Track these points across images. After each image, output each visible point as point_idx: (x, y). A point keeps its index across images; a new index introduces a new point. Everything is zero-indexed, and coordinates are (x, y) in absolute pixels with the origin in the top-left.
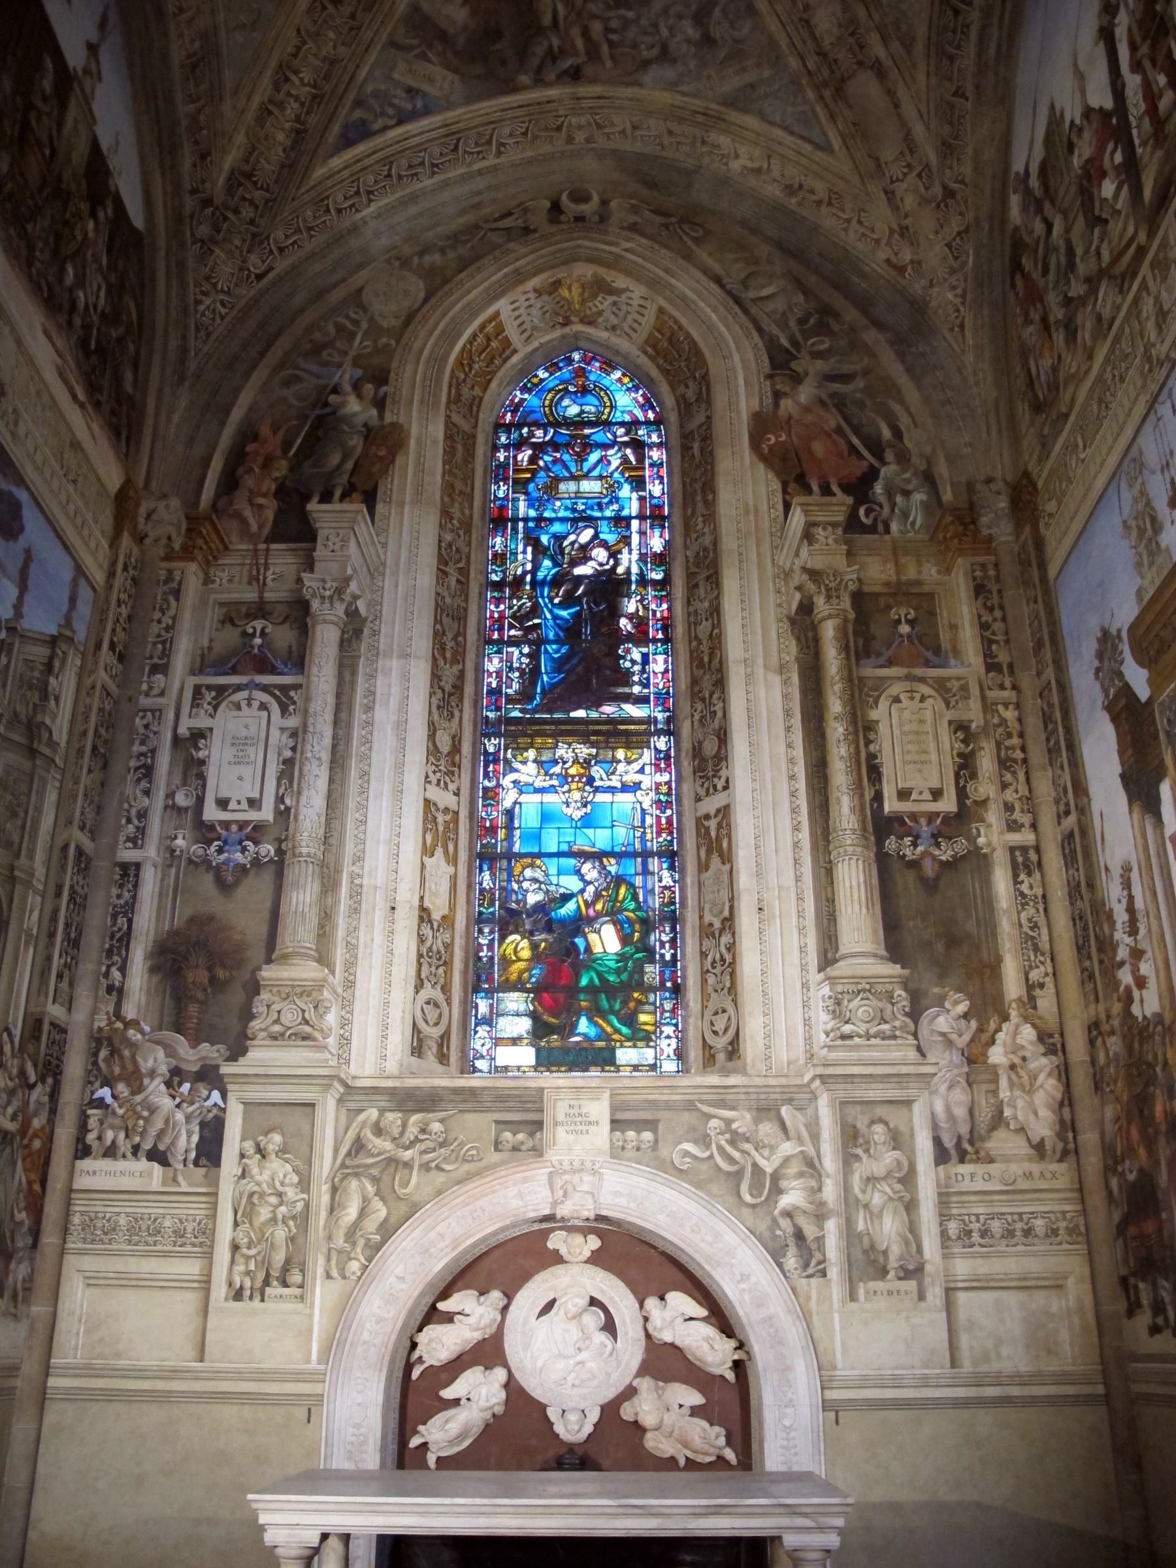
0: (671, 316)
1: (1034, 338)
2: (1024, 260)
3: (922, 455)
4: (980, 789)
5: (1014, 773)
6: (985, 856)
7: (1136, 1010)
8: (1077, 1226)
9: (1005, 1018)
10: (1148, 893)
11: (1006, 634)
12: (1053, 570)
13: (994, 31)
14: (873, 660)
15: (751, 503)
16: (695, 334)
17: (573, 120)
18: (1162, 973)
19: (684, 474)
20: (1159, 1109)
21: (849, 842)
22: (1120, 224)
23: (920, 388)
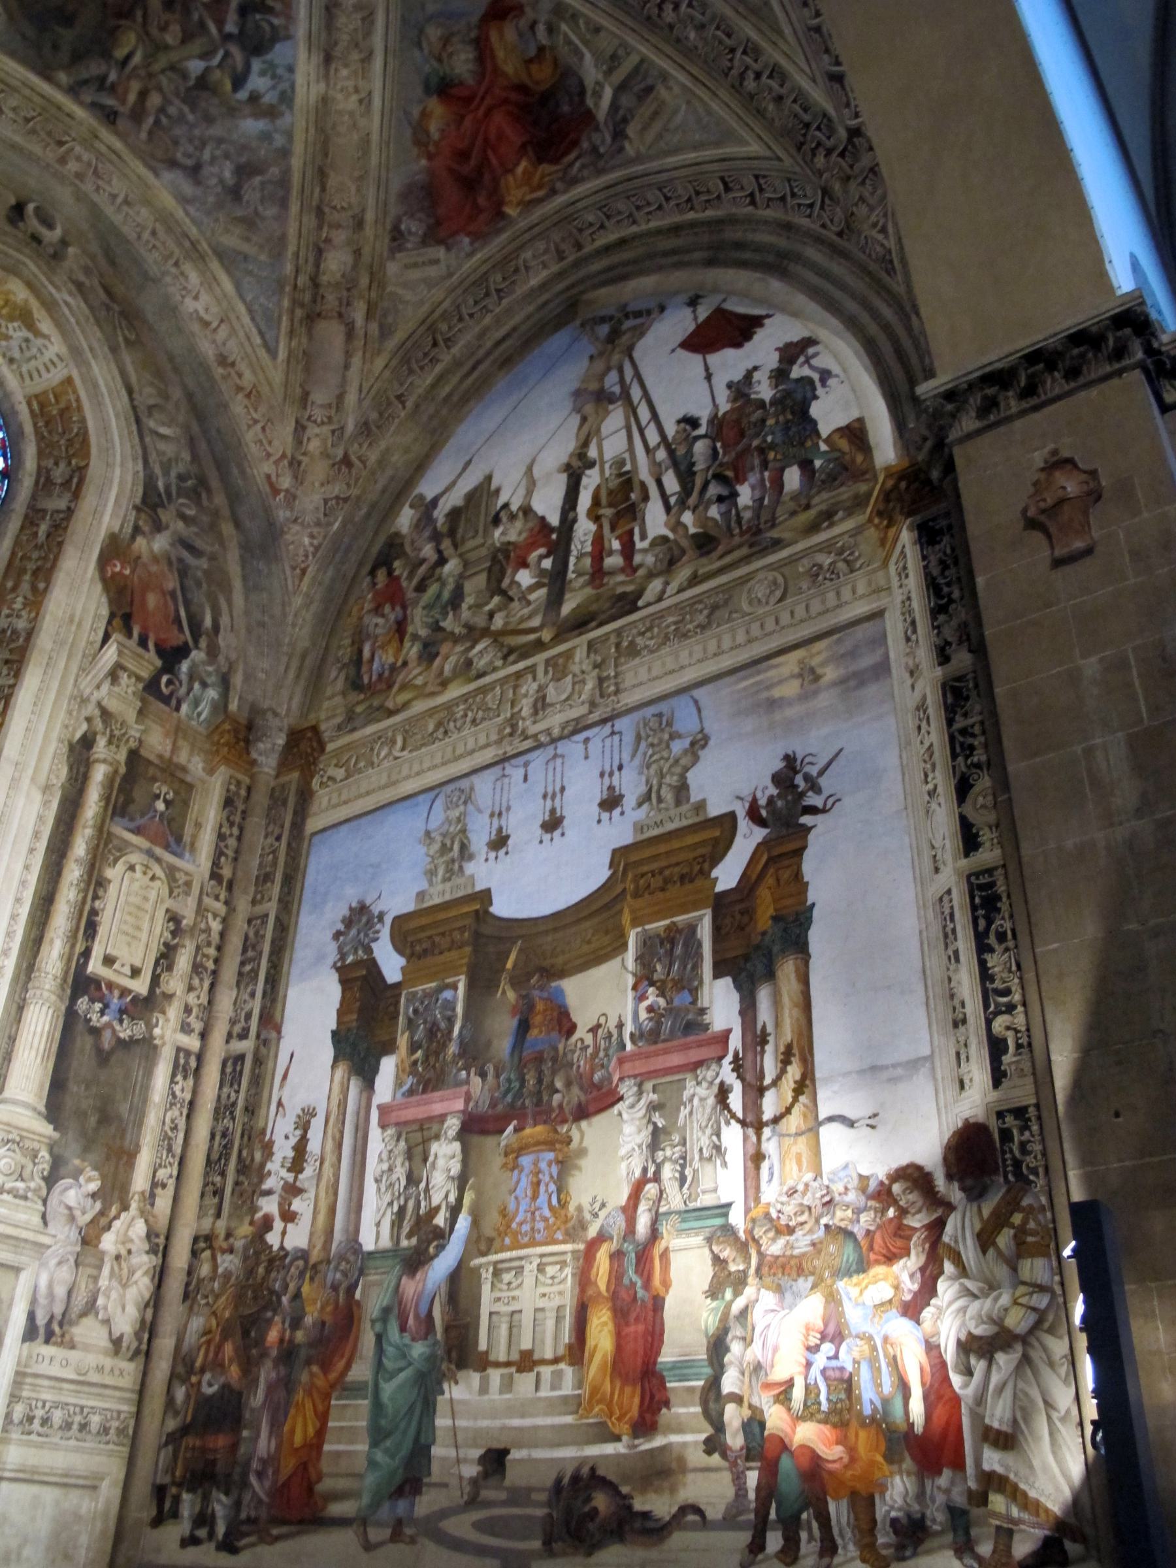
0: (75, 391)
1: (379, 631)
2: (397, 564)
3: (227, 658)
4: (172, 983)
5: (201, 980)
6: (156, 1047)
7: (273, 1239)
8: (126, 1427)
9: (125, 1207)
10: (330, 1144)
11: (237, 852)
12: (313, 824)
13: (455, 380)
14: (125, 821)
15: (78, 613)
16: (91, 424)
17: (78, 149)
18: (322, 1218)
19: (17, 543)
20: (273, 1335)
21: (47, 987)
22: (526, 611)
23: (247, 599)
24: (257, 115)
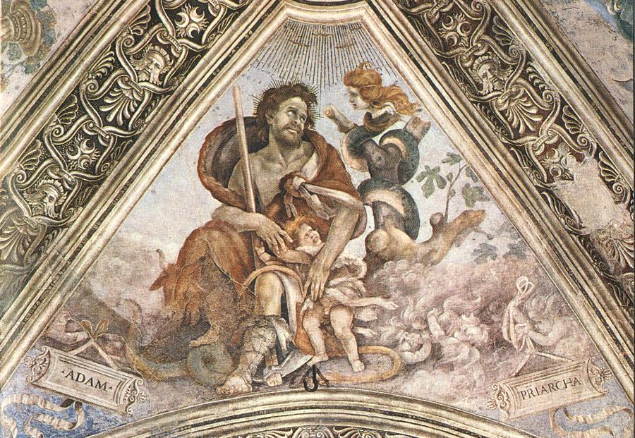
24: (456, 242)
